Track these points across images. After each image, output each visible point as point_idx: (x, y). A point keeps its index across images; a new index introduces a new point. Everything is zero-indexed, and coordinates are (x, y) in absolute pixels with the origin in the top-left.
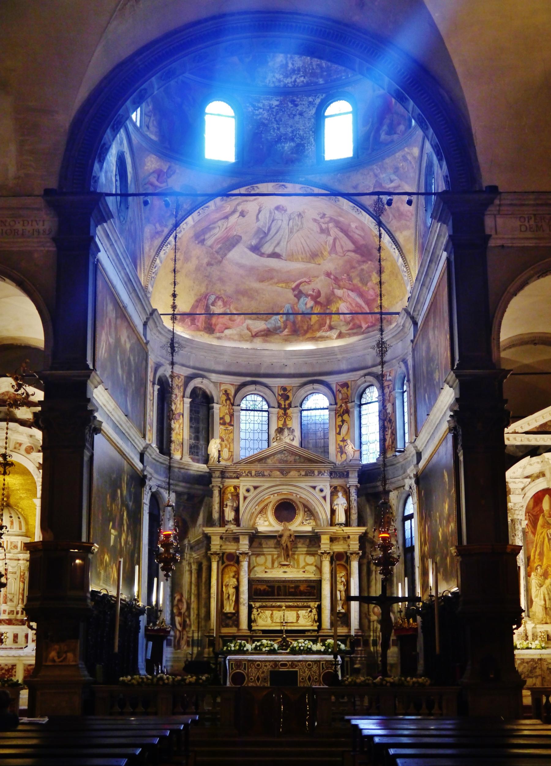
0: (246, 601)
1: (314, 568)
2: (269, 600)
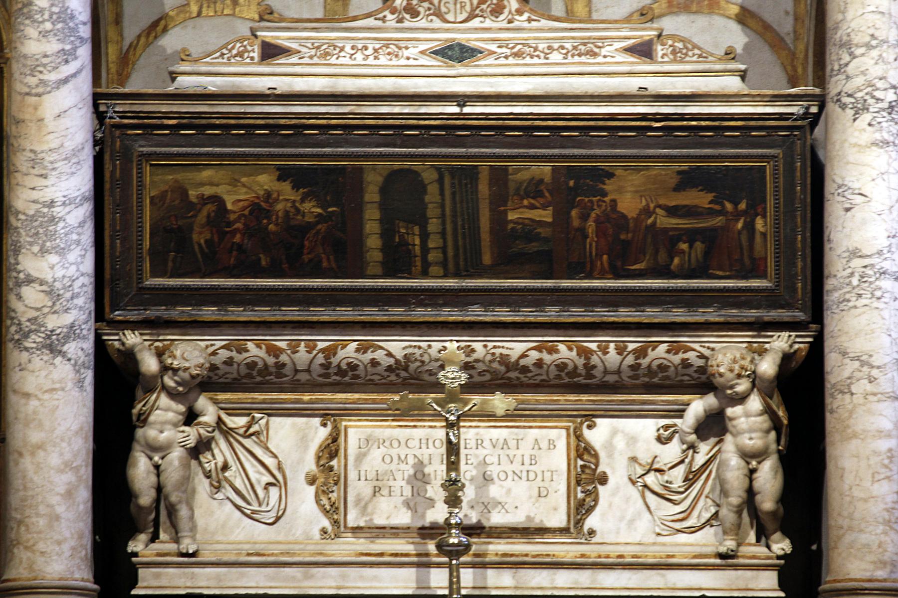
0: (78, 310)
1: (736, 37)
2: (304, 312)
